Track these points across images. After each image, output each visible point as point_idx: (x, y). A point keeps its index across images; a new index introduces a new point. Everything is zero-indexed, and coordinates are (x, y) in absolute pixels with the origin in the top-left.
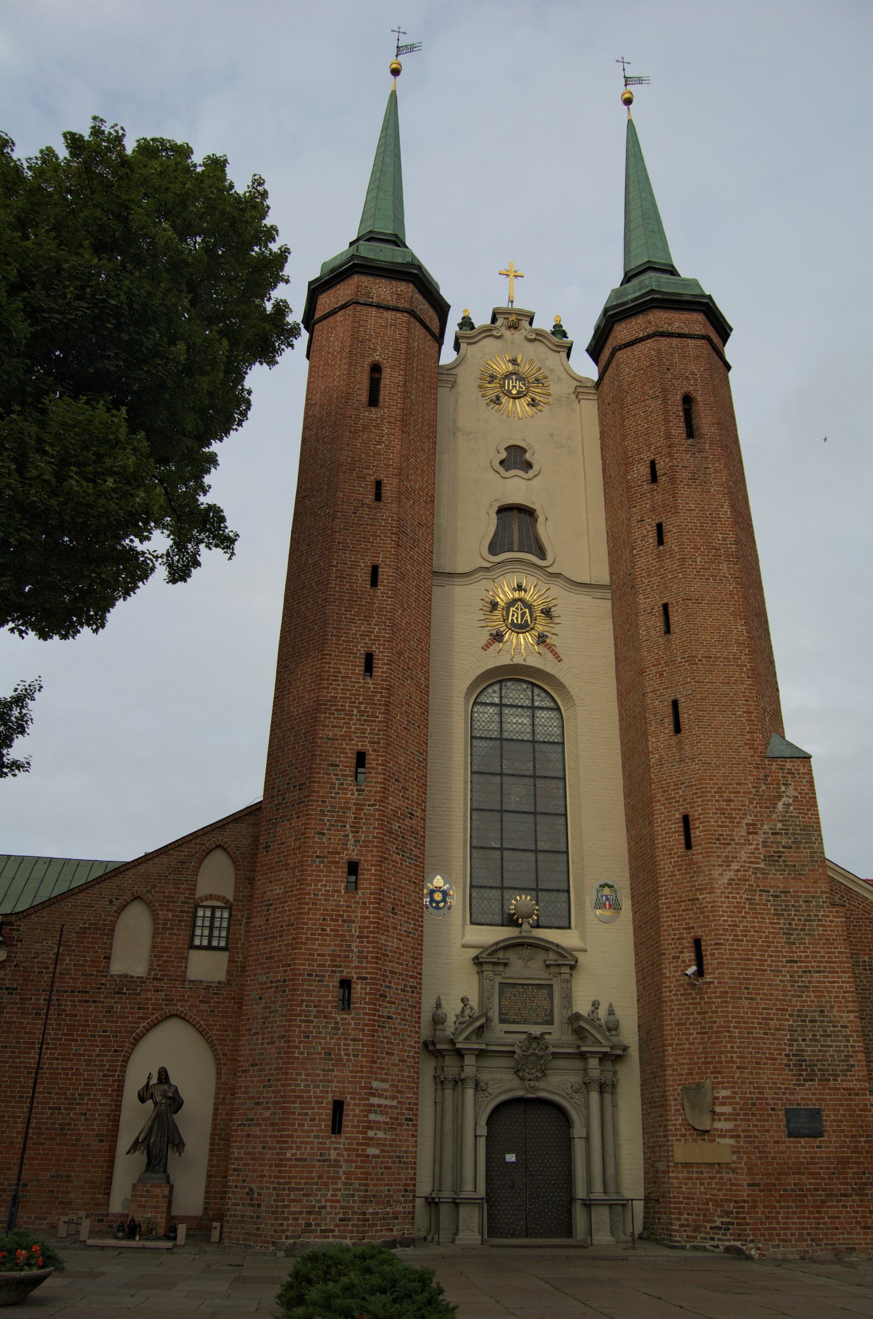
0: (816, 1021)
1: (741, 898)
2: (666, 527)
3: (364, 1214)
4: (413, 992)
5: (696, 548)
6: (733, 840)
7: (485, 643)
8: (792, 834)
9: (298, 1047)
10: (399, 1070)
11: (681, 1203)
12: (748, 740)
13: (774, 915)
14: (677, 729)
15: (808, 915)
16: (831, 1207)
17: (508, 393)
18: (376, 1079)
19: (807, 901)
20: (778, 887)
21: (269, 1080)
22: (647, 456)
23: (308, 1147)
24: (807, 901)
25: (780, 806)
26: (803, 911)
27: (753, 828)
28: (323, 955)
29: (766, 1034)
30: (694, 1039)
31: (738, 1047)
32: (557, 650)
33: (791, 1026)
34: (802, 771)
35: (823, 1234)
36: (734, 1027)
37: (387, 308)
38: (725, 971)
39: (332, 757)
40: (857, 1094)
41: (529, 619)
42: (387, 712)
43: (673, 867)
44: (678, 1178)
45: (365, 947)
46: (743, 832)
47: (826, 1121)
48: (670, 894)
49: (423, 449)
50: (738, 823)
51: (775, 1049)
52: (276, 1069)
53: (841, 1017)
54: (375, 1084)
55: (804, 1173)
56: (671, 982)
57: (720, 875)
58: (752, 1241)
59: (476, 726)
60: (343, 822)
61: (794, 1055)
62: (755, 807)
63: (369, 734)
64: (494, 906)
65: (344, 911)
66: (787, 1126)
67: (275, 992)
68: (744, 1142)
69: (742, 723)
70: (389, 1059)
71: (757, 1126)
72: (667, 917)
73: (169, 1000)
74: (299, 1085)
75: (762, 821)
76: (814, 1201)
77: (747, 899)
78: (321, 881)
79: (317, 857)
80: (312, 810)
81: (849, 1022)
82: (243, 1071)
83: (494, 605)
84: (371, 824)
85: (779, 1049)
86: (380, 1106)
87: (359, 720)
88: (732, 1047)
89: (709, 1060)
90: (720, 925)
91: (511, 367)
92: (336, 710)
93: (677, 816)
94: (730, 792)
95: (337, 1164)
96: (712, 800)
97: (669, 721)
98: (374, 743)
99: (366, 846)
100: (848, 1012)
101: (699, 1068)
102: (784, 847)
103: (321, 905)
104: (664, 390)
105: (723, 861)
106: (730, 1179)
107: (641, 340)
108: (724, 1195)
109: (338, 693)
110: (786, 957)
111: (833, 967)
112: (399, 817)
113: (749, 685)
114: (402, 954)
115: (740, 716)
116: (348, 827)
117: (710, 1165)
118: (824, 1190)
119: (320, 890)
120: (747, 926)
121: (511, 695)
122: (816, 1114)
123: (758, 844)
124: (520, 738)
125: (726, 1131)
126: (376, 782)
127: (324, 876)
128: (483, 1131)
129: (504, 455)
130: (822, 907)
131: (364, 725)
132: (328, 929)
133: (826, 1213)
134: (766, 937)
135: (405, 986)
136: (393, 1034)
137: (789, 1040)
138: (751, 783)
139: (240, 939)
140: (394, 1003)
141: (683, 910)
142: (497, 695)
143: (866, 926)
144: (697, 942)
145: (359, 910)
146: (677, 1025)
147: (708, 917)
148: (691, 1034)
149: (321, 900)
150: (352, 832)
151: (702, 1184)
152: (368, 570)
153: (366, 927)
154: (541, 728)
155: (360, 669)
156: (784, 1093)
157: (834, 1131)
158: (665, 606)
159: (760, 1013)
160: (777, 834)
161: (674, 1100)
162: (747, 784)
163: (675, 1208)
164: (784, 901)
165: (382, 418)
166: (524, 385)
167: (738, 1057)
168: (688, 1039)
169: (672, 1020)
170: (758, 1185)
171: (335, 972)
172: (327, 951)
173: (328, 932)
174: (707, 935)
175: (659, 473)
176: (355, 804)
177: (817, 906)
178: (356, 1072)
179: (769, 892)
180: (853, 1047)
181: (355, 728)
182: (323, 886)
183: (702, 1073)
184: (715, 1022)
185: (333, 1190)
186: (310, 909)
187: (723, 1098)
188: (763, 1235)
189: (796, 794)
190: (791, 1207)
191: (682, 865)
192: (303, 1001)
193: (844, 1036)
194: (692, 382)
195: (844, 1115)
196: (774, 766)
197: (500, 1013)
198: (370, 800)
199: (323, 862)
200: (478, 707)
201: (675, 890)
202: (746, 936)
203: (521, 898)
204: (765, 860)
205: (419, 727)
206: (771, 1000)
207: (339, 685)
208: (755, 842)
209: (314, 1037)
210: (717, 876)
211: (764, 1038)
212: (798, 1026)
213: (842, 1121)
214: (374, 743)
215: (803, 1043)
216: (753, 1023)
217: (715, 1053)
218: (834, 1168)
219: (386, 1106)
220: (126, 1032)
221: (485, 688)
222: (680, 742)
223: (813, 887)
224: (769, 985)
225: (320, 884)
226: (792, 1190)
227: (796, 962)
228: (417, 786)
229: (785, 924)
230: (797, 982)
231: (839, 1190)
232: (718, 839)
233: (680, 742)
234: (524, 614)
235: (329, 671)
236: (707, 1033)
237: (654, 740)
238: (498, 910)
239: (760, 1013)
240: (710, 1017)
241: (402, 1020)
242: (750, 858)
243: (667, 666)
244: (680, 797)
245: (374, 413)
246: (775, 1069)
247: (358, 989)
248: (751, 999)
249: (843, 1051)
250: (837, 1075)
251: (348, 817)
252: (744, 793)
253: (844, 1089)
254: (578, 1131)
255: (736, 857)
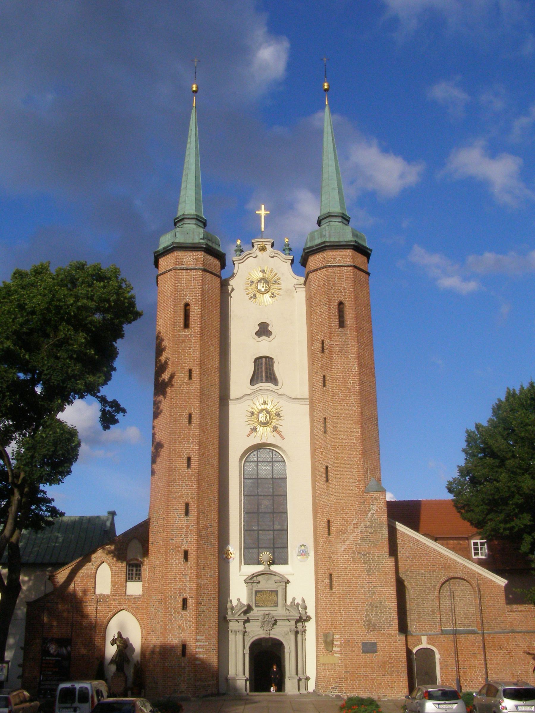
0: (378, 607)
1: (349, 556)
2: (327, 378)
3: (196, 685)
4: (214, 600)
5: (339, 389)
6: (347, 531)
7: (248, 433)
8: (374, 527)
9: (168, 625)
10: (209, 631)
11: (321, 678)
12: (357, 485)
13: (363, 563)
14: (327, 481)
15: (378, 563)
16: (378, 680)
17: (260, 292)
18: (199, 636)
19: (378, 557)
20: (366, 551)
21: (158, 637)
22: (320, 337)
23: (174, 662)
24: (378, 557)
25: (370, 514)
26: (377, 561)
27: (356, 526)
28: (176, 589)
29: (355, 613)
30: (328, 615)
31: (344, 619)
32: (282, 434)
33: (367, 609)
34: (381, 497)
35: (374, 690)
36: (343, 610)
37: (191, 269)
38: (340, 587)
39: (175, 506)
40: (392, 636)
41: (269, 419)
42: (198, 484)
43: (323, 542)
44: (321, 669)
45: (192, 585)
46: (352, 527)
47: (379, 647)
48: (322, 554)
49: (212, 344)
50: (350, 523)
51: (359, 619)
52: (160, 633)
53: (389, 605)
54: (198, 637)
55: (368, 667)
56: (321, 591)
57: (341, 547)
58: (345, 693)
59: (246, 473)
60: (181, 534)
61: (367, 621)
62: (358, 516)
63: (191, 494)
64: (254, 556)
65: (183, 571)
66: (362, 649)
67: (158, 603)
68: (344, 656)
69: (355, 477)
70: (204, 627)
71: (349, 649)
72: (320, 564)
73: (120, 604)
74: (169, 639)
75: (361, 522)
76: (371, 678)
77: (351, 557)
78: (173, 559)
79: (171, 549)
80: (169, 529)
81: (392, 607)
82: (149, 633)
83: (253, 413)
84: (192, 534)
85: (361, 619)
86: (200, 645)
87: (186, 488)
88: (341, 619)
89: (333, 623)
90: (339, 568)
91: (261, 275)
92: (176, 485)
93: (326, 520)
94: (347, 510)
95: (184, 668)
96: (339, 514)
97: (324, 475)
98: (192, 498)
99: (191, 543)
100: (392, 603)
101: (329, 626)
102: (370, 533)
103: (174, 569)
104: (329, 300)
105: (342, 541)
106: (338, 670)
107: (320, 269)
108: (336, 676)
109: (176, 477)
110: (367, 581)
111: (387, 584)
112: (205, 529)
113: (360, 458)
114: (209, 586)
115: (354, 474)
116: (183, 536)
117: (332, 664)
118: (376, 673)
119: (173, 563)
120: (351, 568)
121: (262, 456)
122: (374, 644)
123: (358, 533)
124: (266, 477)
125: (338, 651)
126: (194, 516)
127: (175, 557)
128: (247, 651)
129: (257, 328)
130: (385, 558)
131: (187, 490)
132: (177, 578)
133: (376, 682)
134: (359, 573)
135: (210, 598)
136: (205, 617)
137: (365, 615)
138: (357, 505)
139: (146, 577)
140: (205, 605)
141: (326, 561)
142: (256, 456)
143: (424, 557)
144: (331, 575)
145: (189, 570)
146: (323, 609)
147: (335, 565)
148: (327, 613)
149: (173, 567)
150: (185, 538)
151: (329, 671)
152: (187, 416)
153: (192, 577)
154: (276, 471)
155: (185, 465)
156: (362, 636)
157: (382, 651)
158: (325, 419)
159: (354, 605)
160: (367, 527)
161: (321, 639)
162: (355, 505)
163: (320, 680)
164: (368, 557)
165: (191, 334)
166: (268, 285)
167: (343, 622)
168: (326, 615)
169: (321, 607)
170: (349, 672)
171: (180, 595)
172: (177, 587)
173: (177, 579)
174: (335, 573)
175: (325, 347)
176: (186, 526)
177: (383, 558)
178: (190, 633)
179: (361, 553)
180: (392, 617)
181: (185, 492)
182: (174, 561)
183: (330, 628)
184: (335, 608)
185: (184, 677)
186: (169, 571)
187: (337, 638)
188: (349, 691)
189: (377, 509)
190: (362, 680)
191: (326, 542)
192: (169, 607)
193: (389, 613)
194: (343, 294)
195: (386, 644)
196: (369, 496)
197: (256, 603)
198: (192, 524)
199: (174, 551)
200: (247, 463)
201: (323, 552)
202: (350, 572)
203: (264, 553)
204: (361, 539)
205: (213, 486)
206: (359, 599)
207: (177, 473)
208: (357, 532)
209: (174, 621)
210: (339, 548)
211: (354, 615)
212: (370, 609)
213: (385, 647)
214: (192, 498)
215: (371, 616)
216: (350, 608)
217: (335, 620)
218: (381, 665)
219: (203, 645)
220: (104, 617)
221: (251, 453)
222: (328, 486)
223: (381, 550)
224: (359, 593)
225: (173, 560)
226: (363, 674)
227: (371, 583)
228: (213, 512)
229: (367, 567)
230: (371, 591)
231: (382, 673)
232: (341, 531)
233: (328, 486)
234: (266, 417)
235: (172, 467)
236: (332, 613)
237: (318, 484)
238: (256, 558)
239: (354, 605)
240: (334, 606)
241: (209, 611)
242: (354, 538)
243: (324, 449)
244: (327, 511)
245: (187, 332)
246: (358, 627)
247: (190, 602)
248: (351, 599)
249: (388, 619)
250: (385, 629)
251: (183, 532)
252: (354, 509)
253: (387, 634)
254: (287, 651)
255: (348, 539)
